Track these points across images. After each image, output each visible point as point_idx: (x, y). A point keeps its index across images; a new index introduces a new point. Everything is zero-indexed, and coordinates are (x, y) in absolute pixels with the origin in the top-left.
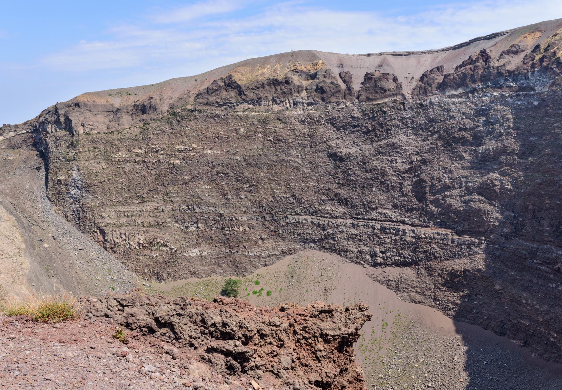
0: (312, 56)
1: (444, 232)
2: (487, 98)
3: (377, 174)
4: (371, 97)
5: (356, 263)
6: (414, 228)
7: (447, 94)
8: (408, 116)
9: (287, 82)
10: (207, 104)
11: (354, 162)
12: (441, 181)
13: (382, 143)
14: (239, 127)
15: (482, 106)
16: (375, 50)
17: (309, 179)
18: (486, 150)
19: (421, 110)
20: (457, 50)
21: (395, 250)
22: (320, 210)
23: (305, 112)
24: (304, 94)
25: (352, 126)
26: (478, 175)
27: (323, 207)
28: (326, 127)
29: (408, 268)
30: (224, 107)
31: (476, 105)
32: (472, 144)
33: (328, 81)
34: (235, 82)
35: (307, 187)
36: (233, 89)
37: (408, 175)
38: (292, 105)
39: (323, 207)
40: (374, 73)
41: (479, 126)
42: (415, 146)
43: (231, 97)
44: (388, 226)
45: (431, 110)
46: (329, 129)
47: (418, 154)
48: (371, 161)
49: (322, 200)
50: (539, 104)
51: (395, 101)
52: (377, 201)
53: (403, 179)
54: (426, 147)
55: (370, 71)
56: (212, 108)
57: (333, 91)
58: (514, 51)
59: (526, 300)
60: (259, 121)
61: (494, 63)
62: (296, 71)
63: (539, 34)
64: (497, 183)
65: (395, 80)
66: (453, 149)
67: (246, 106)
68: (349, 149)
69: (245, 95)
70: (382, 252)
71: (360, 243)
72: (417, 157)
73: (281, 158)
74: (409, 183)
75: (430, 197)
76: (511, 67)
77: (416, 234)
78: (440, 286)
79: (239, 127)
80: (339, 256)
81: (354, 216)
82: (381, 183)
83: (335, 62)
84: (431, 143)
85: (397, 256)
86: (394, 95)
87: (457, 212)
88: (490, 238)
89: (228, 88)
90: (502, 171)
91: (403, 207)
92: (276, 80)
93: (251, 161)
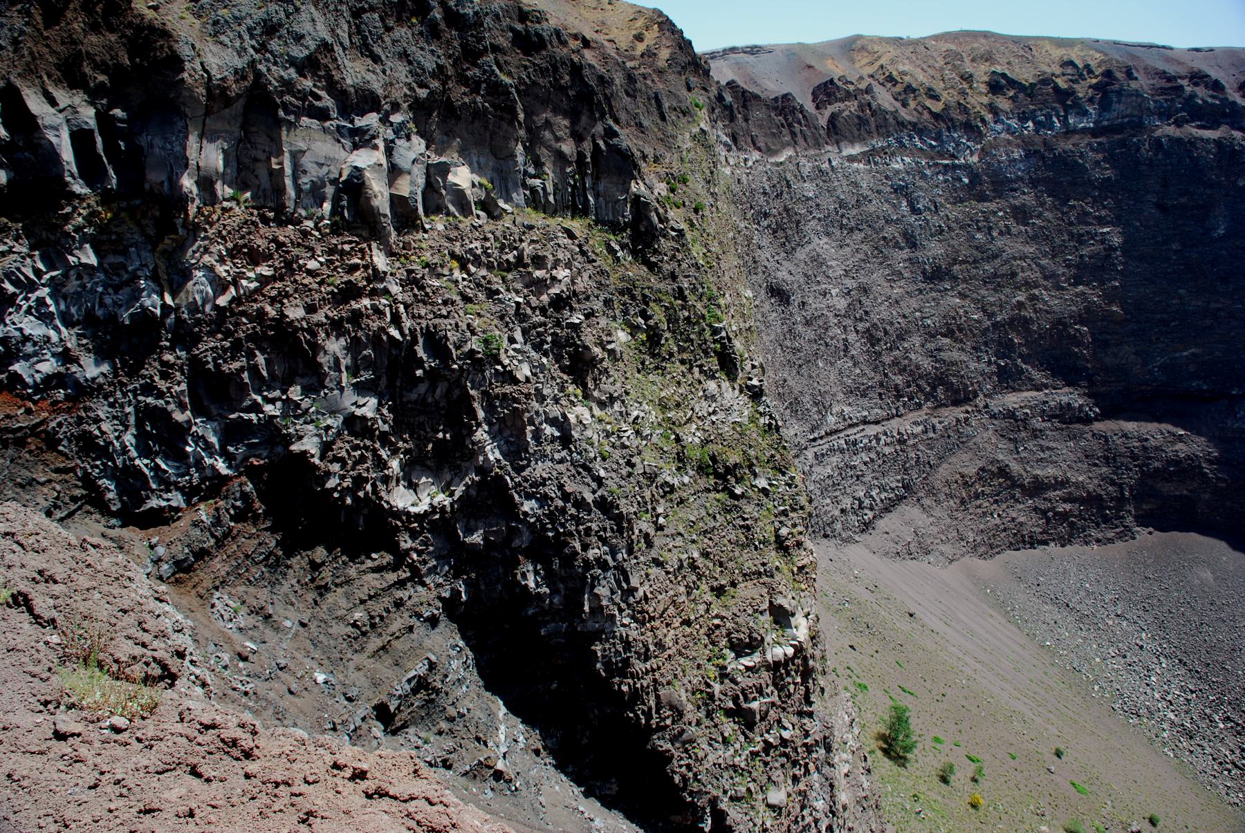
3: (820, 327)
7: (845, 153)
12: (892, 324)
13: (801, 254)
15: (900, 180)
19: (821, 183)
29: (903, 506)
31: (887, 178)
32: (901, 249)
41: (903, 216)
44: (857, 437)
45: (836, 184)
53: (845, 327)
64: (961, 312)
66: (886, 258)
71: (838, 493)
77: (893, 437)
80: (825, 541)
82: (827, 345)
84: (857, 251)
85: (880, 492)
88: (976, 406)
90: (959, 293)
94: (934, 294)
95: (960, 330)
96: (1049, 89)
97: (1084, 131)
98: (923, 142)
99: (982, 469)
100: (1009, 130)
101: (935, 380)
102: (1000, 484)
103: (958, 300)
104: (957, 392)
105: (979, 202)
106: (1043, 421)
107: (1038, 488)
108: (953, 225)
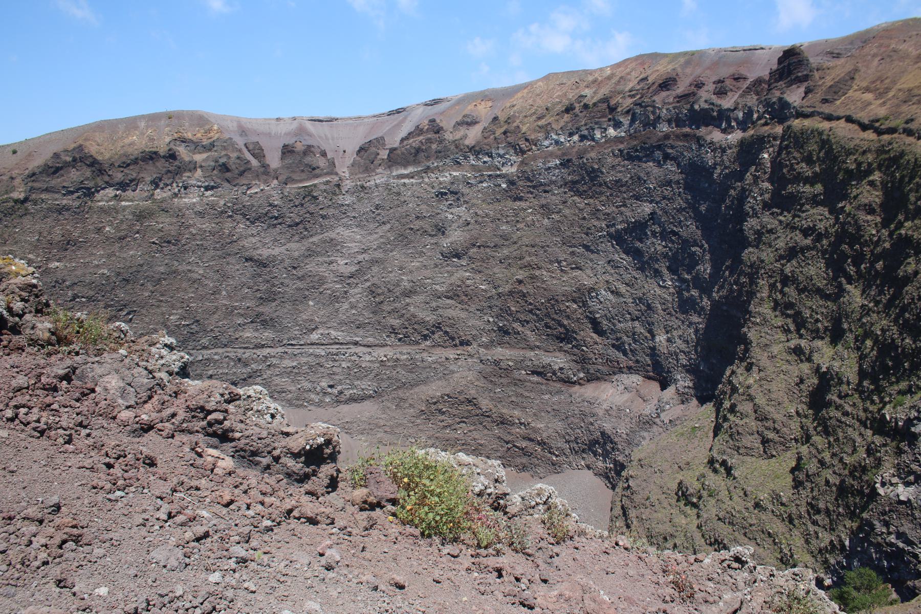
0: (200, 120)
1: (409, 351)
2: (445, 179)
4: (295, 176)
5: (298, 406)
6: (369, 350)
7: (394, 174)
8: (346, 203)
9: (172, 156)
10: (47, 190)
11: (280, 267)
12: (398, 285)
13: (315, 239)
14: (104, 224)
16: (286, 114)
17: (217, 296)
18: (452, 243)
19: (362, 194)
20: (391, 116)
21: (348, 381)
22: (237, 339)
23: (202, 200)
24: (199, 171)
25: (272, 218)
26: (446, 275)
27: (241, 334)
28: (234, 221)
30: (76, 195)
31: (433, 187)
33: (234, 155)
34: (91, 156)
35: (217, 308)
36: (88, 166)
37: (355, 281)
38: (182, 189)
39: (241, 334)
40: (293, 144)
42: (361, 242)
43: (87, 179)
44: (335, 351)
46: (238, 223)
47: (365, 251)
48: (302, 265)
49: (239, 324)
50: (508, 186)
51: (328, 182)
52: (316, 319)
54: (375, 243)
55: (290, 141)
56: (57, 196)
57: (242, 169)
58: (469, 122)
59: (519, 419)
60: (134, 214)
61: (449, 136)
62: (184, 141)
63: (490, 104)
64: (468, 282)
65: (324, 154)
66: (410, 242)
67: (111, 192)
68: (270, 250)
69: (109, 175)
70: (331, 387)
71: (300, 378)
72: (364, 255)
73: (173, 268)
74: (356, 290)
75: (386, 307)
76: (469, 142)
78: (413, 419)
79: (104, 224)
81: (284, 342)
83: (233, 126)
84: (381, 237)
85: (352, 389)
86: (327, 174)
87: (423, 322)
89: (79, 164)
91: (352, 322)
92: (155, 153)
93: (126, 276)
94: (449, 268)
95: (466, 295)
96: (605, 106)
97: (618, 140)
98: (479, 159)
99: (448, 395)
100: (557, 142)
101: (433, 327)
102: (469, 411)
103: (468, 274)
104: (453, 339)
105: (515, 201)
106: (527, 374)
107: (503, 422)
108: (480, 219)
